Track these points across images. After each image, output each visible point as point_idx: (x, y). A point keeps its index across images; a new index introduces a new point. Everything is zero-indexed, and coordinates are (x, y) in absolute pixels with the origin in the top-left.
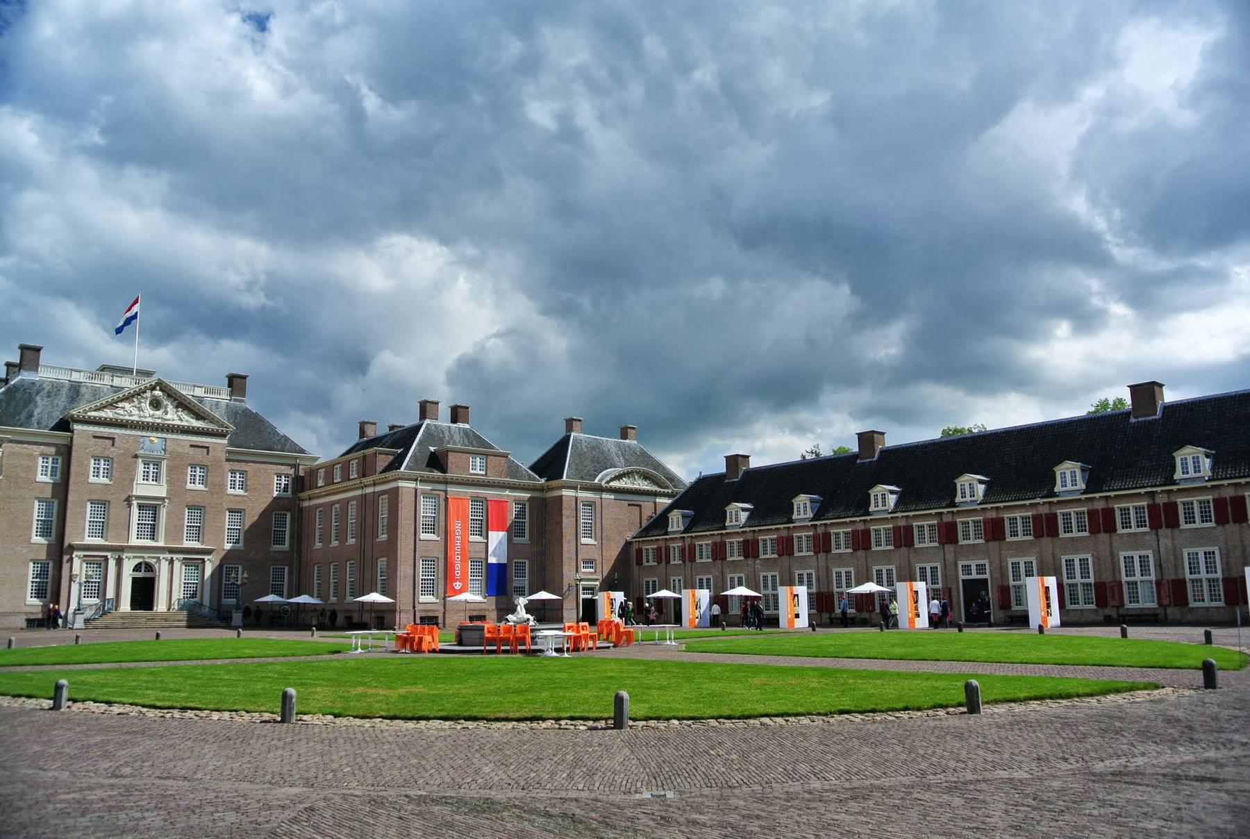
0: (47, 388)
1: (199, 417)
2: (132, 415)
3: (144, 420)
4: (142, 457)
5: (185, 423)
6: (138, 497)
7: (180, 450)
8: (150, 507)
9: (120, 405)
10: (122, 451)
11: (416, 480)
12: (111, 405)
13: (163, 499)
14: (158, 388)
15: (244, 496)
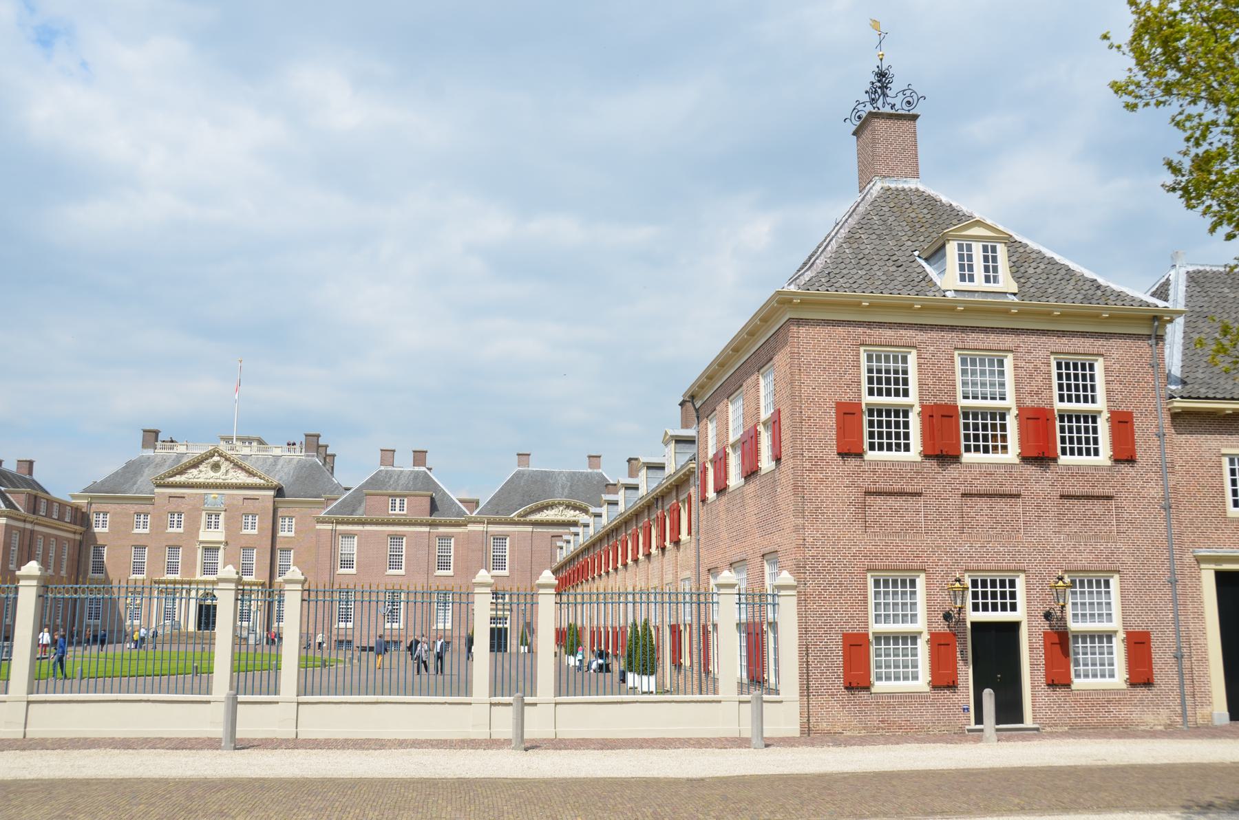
0: (157, 460)
1: (251, 474)
2: (199, 478)
3: (208, 481)
4: (206, 510)
5: (240, 481)
6: (202, 542)
7: (235, 502)
8: (210, 549)
9: (189, 471)
10: (190, 507)
11: (333, 523)
12: (181, 473)
13: (220, 543)
14: (216, 454)
15: (292, 537)
